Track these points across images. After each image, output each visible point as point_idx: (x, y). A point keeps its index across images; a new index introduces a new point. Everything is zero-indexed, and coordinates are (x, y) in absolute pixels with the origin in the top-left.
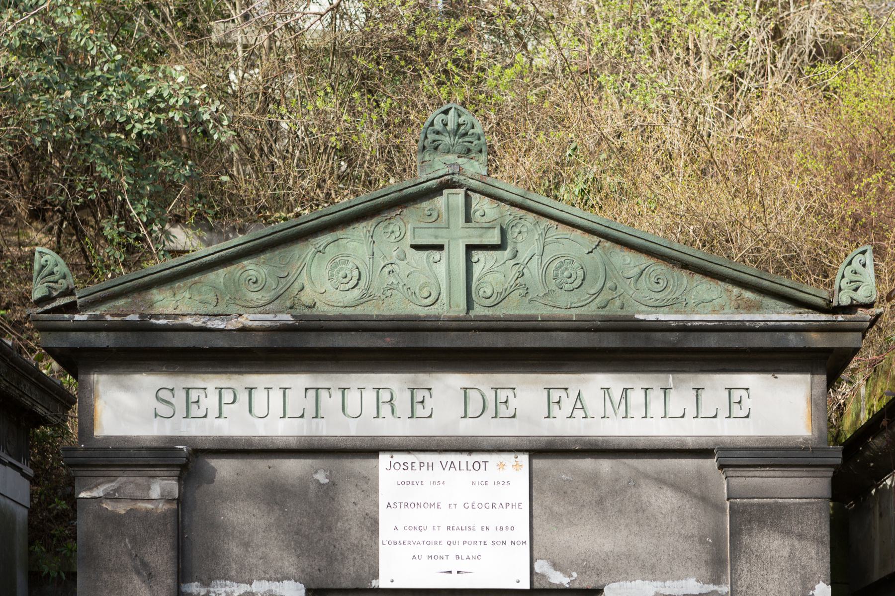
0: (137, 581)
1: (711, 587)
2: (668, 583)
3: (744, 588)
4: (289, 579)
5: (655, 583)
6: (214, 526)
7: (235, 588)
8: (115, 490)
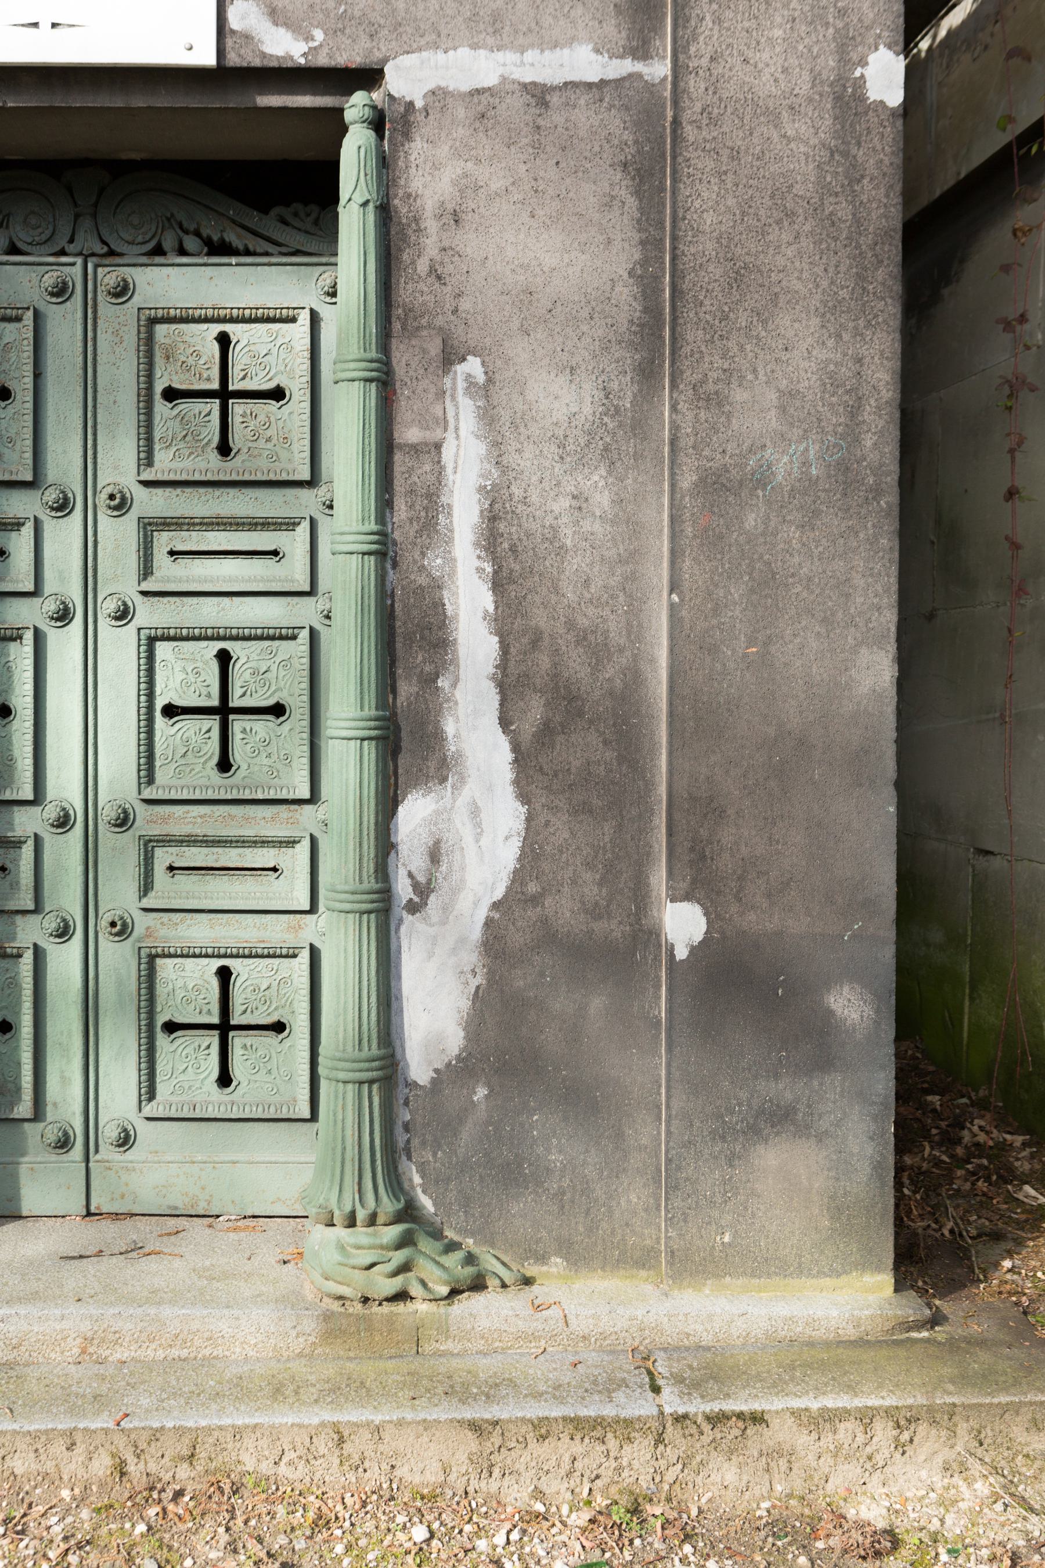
1: (627, 66)
2: (530, 55)
3: (705, 62)
5: (500, 56)
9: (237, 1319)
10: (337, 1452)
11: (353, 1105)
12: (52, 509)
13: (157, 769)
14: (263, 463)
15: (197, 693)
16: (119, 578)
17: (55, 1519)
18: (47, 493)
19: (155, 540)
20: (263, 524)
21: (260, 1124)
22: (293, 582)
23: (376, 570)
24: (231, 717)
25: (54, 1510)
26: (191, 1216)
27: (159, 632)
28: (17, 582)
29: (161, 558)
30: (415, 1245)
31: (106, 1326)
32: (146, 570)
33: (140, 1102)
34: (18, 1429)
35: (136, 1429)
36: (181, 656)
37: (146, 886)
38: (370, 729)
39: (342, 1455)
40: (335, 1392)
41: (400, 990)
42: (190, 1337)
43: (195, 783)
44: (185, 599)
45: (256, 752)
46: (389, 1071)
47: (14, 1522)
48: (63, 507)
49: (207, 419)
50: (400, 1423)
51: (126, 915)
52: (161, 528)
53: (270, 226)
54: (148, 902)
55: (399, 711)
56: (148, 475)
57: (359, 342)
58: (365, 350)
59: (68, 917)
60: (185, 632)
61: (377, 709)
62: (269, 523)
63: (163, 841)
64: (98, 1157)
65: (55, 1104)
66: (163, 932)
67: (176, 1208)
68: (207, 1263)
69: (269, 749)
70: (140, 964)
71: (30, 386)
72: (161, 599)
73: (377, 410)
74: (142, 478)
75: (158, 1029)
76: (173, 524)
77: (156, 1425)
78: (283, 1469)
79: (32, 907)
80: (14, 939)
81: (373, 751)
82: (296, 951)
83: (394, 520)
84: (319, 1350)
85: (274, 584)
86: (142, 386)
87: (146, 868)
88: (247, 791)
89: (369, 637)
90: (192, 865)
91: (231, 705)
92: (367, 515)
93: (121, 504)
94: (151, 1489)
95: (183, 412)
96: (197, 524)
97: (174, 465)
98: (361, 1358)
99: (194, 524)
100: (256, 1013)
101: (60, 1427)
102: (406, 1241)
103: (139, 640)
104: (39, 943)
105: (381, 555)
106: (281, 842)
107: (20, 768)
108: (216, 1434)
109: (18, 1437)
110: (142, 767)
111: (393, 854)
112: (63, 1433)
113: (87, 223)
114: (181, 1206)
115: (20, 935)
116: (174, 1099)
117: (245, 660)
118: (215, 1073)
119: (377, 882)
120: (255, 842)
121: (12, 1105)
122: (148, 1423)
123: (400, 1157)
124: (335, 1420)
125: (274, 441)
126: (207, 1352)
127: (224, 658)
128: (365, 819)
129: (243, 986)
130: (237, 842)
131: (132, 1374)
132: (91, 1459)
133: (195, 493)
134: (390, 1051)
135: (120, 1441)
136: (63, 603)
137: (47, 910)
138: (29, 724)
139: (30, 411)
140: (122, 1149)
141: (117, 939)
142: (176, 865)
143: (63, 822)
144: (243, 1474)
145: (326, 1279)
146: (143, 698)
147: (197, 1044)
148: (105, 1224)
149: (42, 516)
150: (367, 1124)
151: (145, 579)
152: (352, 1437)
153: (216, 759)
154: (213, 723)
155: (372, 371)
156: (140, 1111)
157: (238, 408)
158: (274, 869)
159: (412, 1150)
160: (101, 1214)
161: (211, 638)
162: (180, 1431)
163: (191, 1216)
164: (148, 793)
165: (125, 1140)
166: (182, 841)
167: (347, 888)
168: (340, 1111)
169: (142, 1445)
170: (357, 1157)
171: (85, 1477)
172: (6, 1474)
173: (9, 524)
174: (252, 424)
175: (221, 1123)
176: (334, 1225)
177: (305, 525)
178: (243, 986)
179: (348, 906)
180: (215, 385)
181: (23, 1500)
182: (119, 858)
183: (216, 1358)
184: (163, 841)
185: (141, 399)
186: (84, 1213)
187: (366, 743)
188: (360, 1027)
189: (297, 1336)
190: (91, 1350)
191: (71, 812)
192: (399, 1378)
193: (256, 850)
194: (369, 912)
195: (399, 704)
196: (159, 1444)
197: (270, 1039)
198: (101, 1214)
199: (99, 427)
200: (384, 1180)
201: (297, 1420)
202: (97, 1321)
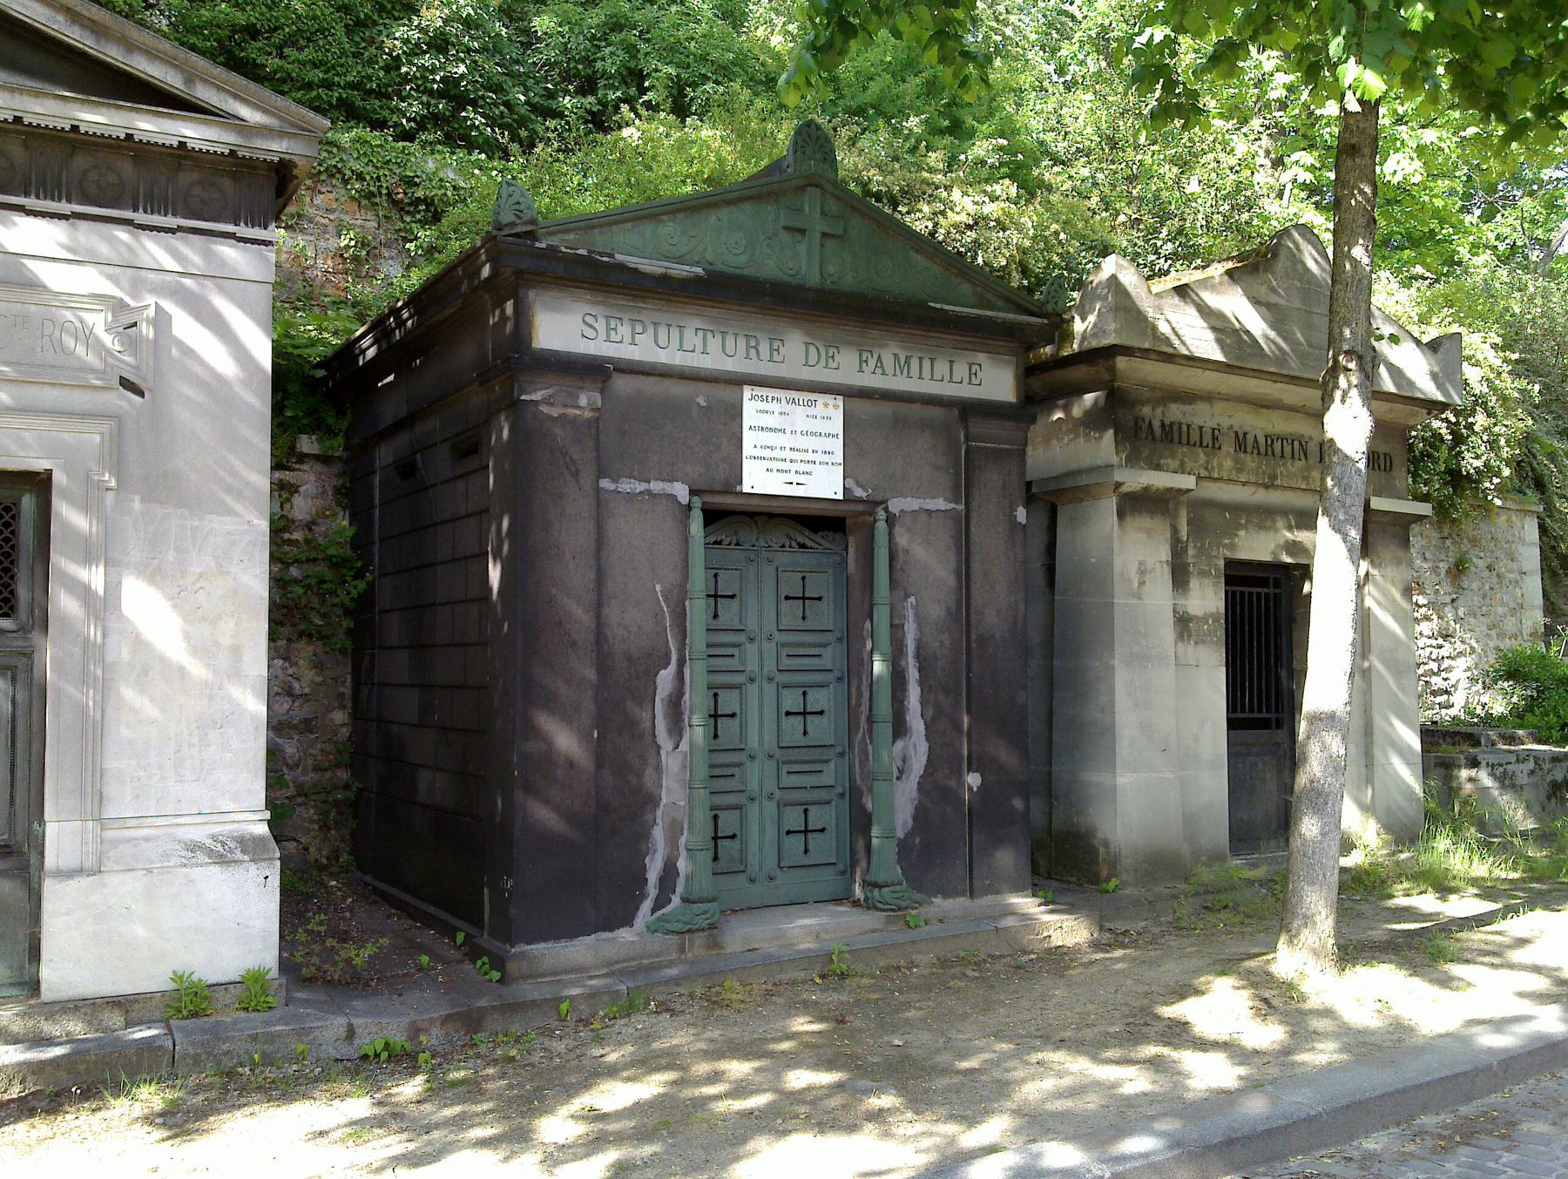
29: (784, 657)
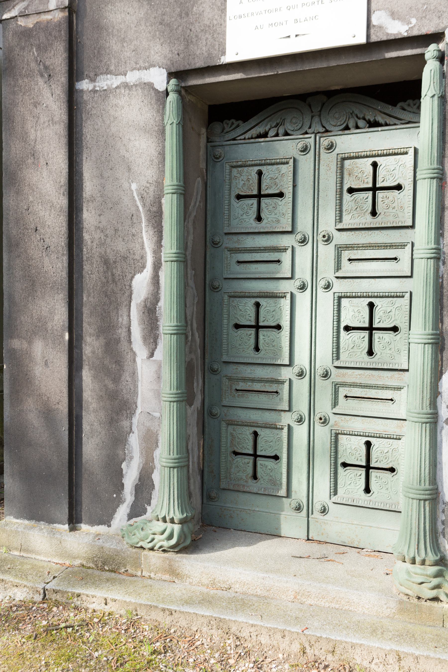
0: (41, 82)
4: (154, 66)
6: (99, 27)
7: (114, 80)
8: (26, 8)
9: (360, 596)
10: (398, 664)
11: (416, 509)
12: (300, 242)
13: (341, 353)
14: (391, 219)
15: (359, 321)
16: (327, 271)
17: (274, 666)
18: (297, 236)
19: (342, 254)
20: (390, 246)
21: (383, 511)
22: (403, 271)
23: (434, 266)
24: (374, 332)
25: (274, 662)
26: (352, 547)
27: (343, 294)
28: (284, 273)
29: (345, 262)
30: (444, 577)
31: (304, 588)
32: (338, 267)
33: (330, 495)
34: (263, 625)
35: (310, 635)
36: (352, 305)
37: (335, 403)
38: (429, 339)
39: (400, 666)
40: (400, 636)
41: (441, 460)
42: (340, 600)
43: (357, 360)
44: (355, 280)
45: (384, 348)
46: (435, 496)
47: (258, 663)
48: (304, 241)
49: (366, 200)
50: (427, 657)
51: (326, 415)
52: (345, 249)
53: (396, 111)
54: (336, 410)
55: (444, 331)
56: (340, 226)
57: (428, 161)
58: (431, 164)
59: (302, 414)
60: (354, 294)
61: (432, 330)
62: (393, 246)
63: (343, 385)
64: (313, 516)
65: (295, 492)
66: (342, 424)
67: (345, 543)
68: (353, 569)
69: (390, 346)
70: (331, 437)
71: (291, 191)
72: (344, 280)
73: (436, 192)
74: (337, 228)
75: (339, 465)
76: (350, 247)
77: (319, 635)
78: (373, 666)
79: (288, 409)
80: (280, 422)
81: (430, 349)
82: (400, 437)
83: (444, 242)
84: (397, 616)
85: (394, 273)
86: (338, 188)
87: (335, 396)
88: (380, 365)
89: (430, 297)
90: (355, 396)
91: (374, 326)
92: (430, 241)
93: (328, 239)
94: (316, 662)
95: (356, 198)
96: (361, 247)
97: (351, 221)
98: (415, 624)
99: (359, 247)
100: (382, 463)
101: (279, 628)
102: (439, 575)
103: (334, 298)
104: (290, 424)
105: (437, 259)
106: (394, 388)
107: (284, 351)
108: (344, 644)
109: (263, 629)
110: (334, 353)
111: (439, 397)
112: (280, 631)
113: (316, 119)
114: (347, 542)
115: (283, 420)
116: (345, 496)
117: (381, 306)
118: (363, 487)
119: (430, 409)
120: (383, 387)
121: (278, 490)
122: (315, 634)
123: (440, 536)
124: (397, 649)
125: (396, 209)
126: (347, 608)
127: (371, 306)
128: (425, 380)
129: (376, 450)
130: (375, 387)
131: (313, 611)
132: (291, 643)
133: (360, 233)
134: (436, 487)
135: (304, 639)
136: (303, 282)
137: (294, 411)
138: (288, 333)
139: (291, 202)
140: (323, 514)
141: (322, 425)
142: (348, 395)
143: (301, 374)
144: (355, 664)
145: (401, 585)
146: (335, 323)
147: (355, 473)
148: (315, 545)
149: (295, 246)
150: (423, 519)
151: (337, 271)
152: (405, 659)
153: (366, 350)
154: (366, 334)
155: (434, 174)
156: (330, 499)
157: (380, 195)
158: (392, 400)
159: (446, 533)
160: (314, 540)
161: (366, 297)
162: (329, 640)
163: (352, 547)
164: (337, 364)
165: (324, 511)
166: (351, 385)
167: (416, 411)
168: (410, 512)
169: (313, 643)
170: (417, 533)
171: (289, 651)
172: (258, 642)
173: (282, 249)
174: (386, 201)
175: (365, 509)
176: (405, 562)
177: (410, 246)
178: (376, 450)
179: (416, 420)
180: (370, 185)
181: (263, 655)
182: (324, 389)
183: (350, 611)
184: (343, 385)
185: (338, 193)
186: (307, 539)
187: (427, 345)
188: (420, 475)
189: (387, 608)
190: (298, 597)
191: (304, 370)
192: (431, 636)
193: (383, 391)
194: (426, 423)
195: (444, 327)
196: (319, 643)
197: (388, 474)
198: (314, 540)
199: (319, 207)
200: (430, 545)
201: (380, 646)
202: (301, 586)
